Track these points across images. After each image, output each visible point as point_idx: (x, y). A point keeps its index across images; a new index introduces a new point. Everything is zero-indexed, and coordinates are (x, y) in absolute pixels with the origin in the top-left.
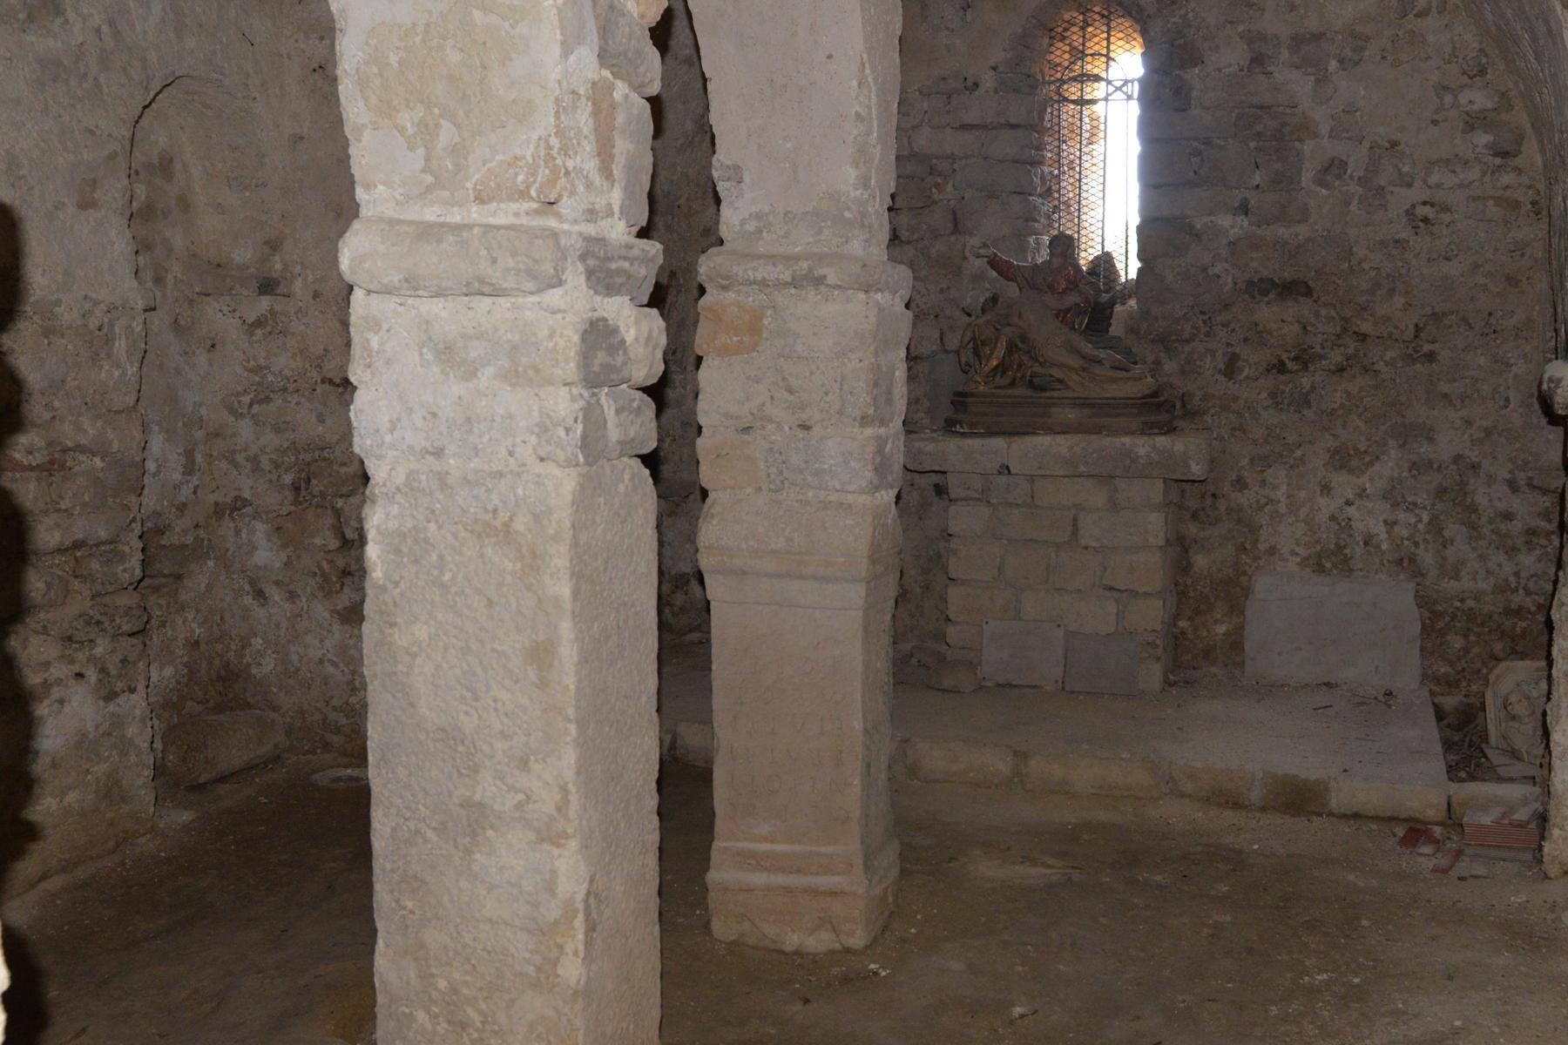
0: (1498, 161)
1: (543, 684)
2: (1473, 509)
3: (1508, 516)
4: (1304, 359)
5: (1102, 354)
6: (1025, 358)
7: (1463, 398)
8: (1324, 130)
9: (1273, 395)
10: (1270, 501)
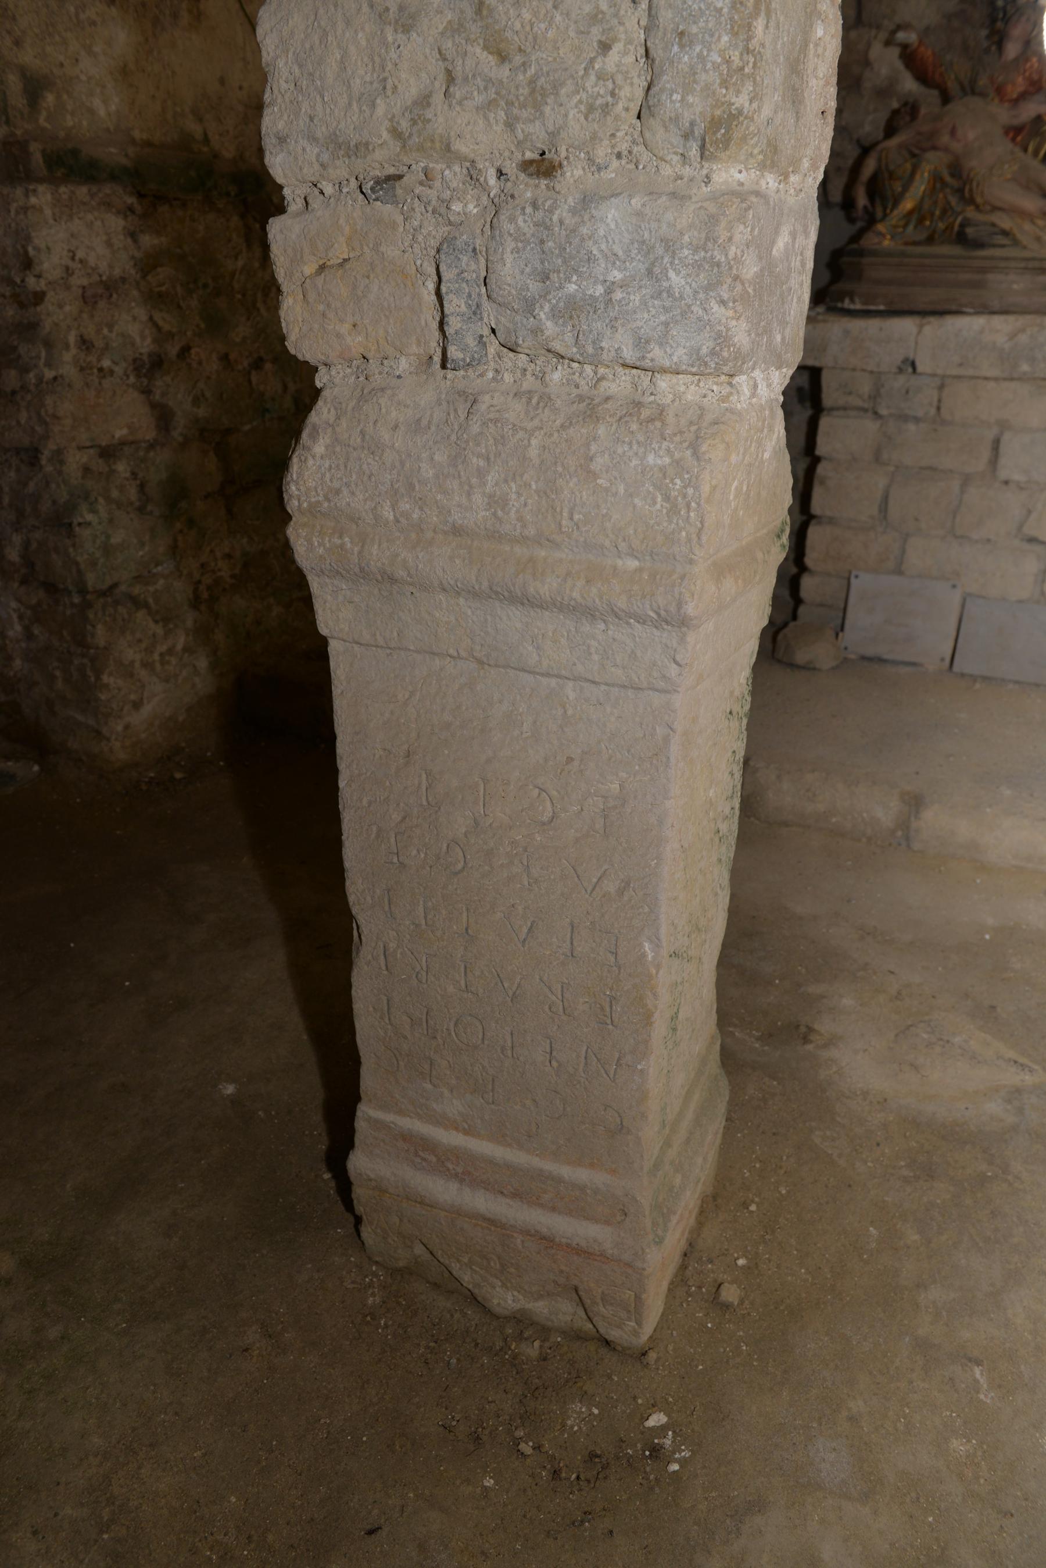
6: (953, 200)
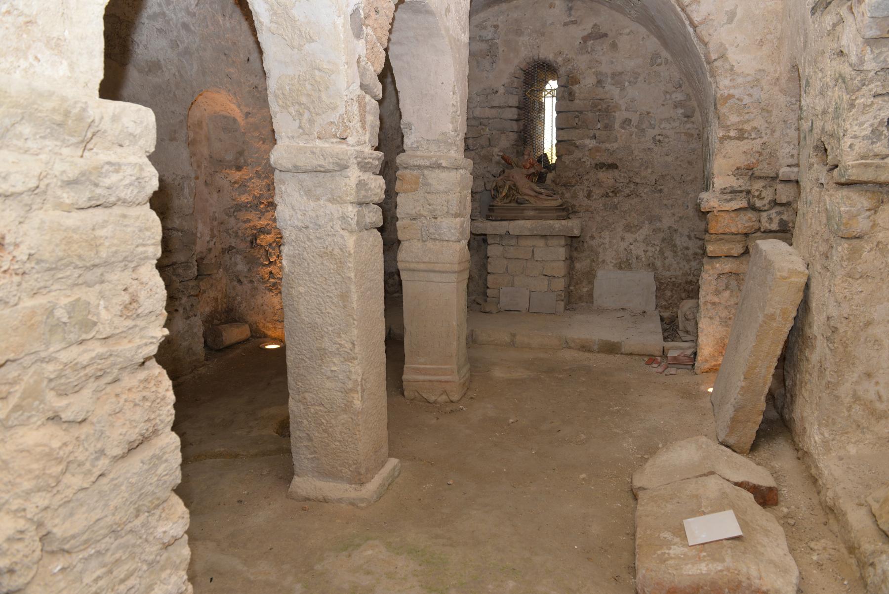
0: (686, 119)
1: (345, 307)
2: (675, 246)
3: (687, 248)
4: (615, 192)
5: (543, 191)
7: (672, 206)
8: (623, 108)
9: (604, 205)
10: (603, 244)
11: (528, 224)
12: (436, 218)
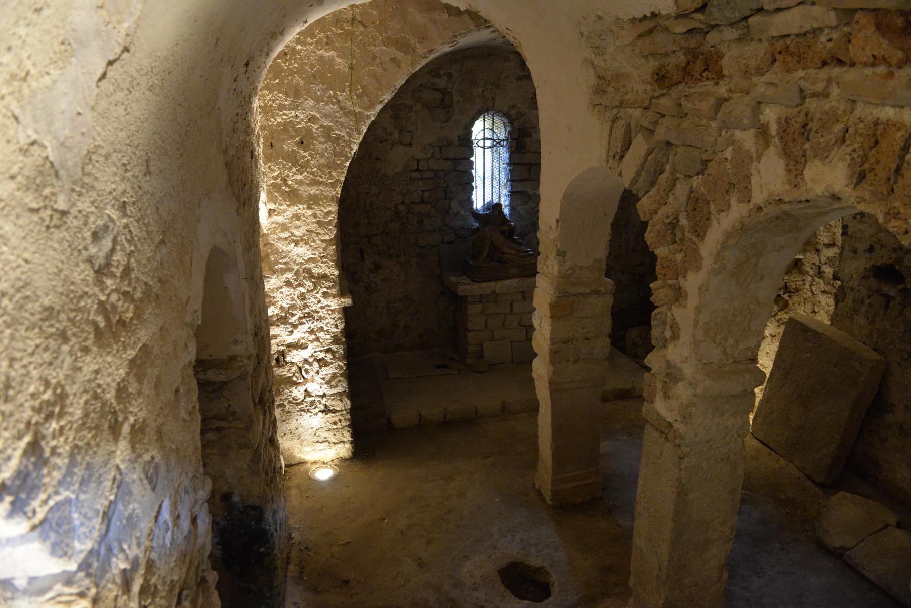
11: (513, 282)
12: (588, 339)
